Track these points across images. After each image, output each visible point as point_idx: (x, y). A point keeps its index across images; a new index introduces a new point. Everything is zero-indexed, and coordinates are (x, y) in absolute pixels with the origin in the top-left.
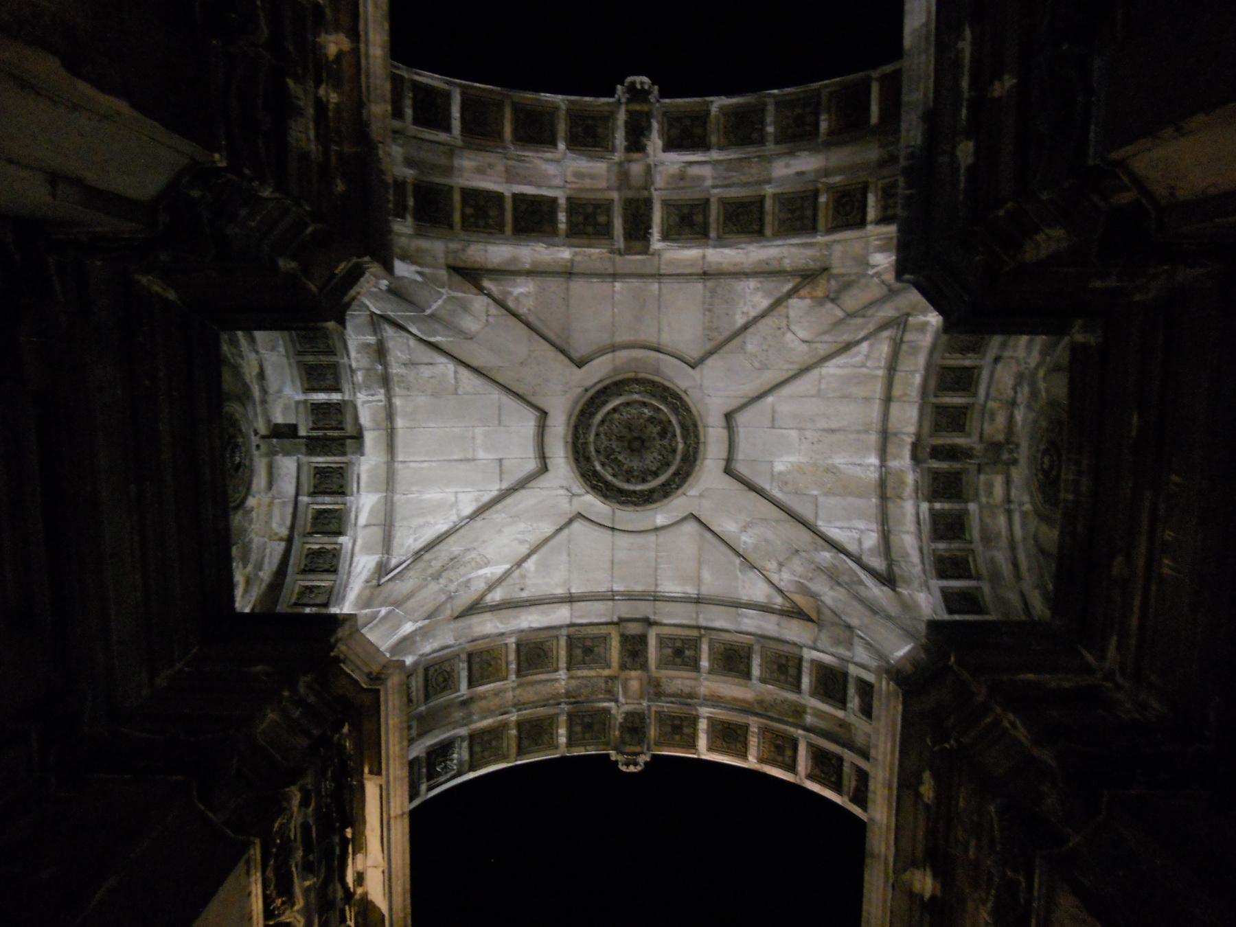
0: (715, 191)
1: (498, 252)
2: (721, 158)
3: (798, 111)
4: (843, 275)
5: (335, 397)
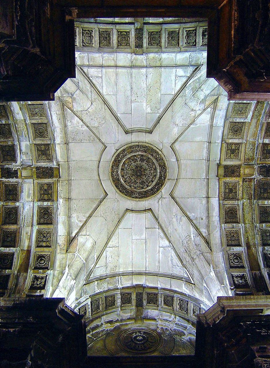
1: (61, 230)
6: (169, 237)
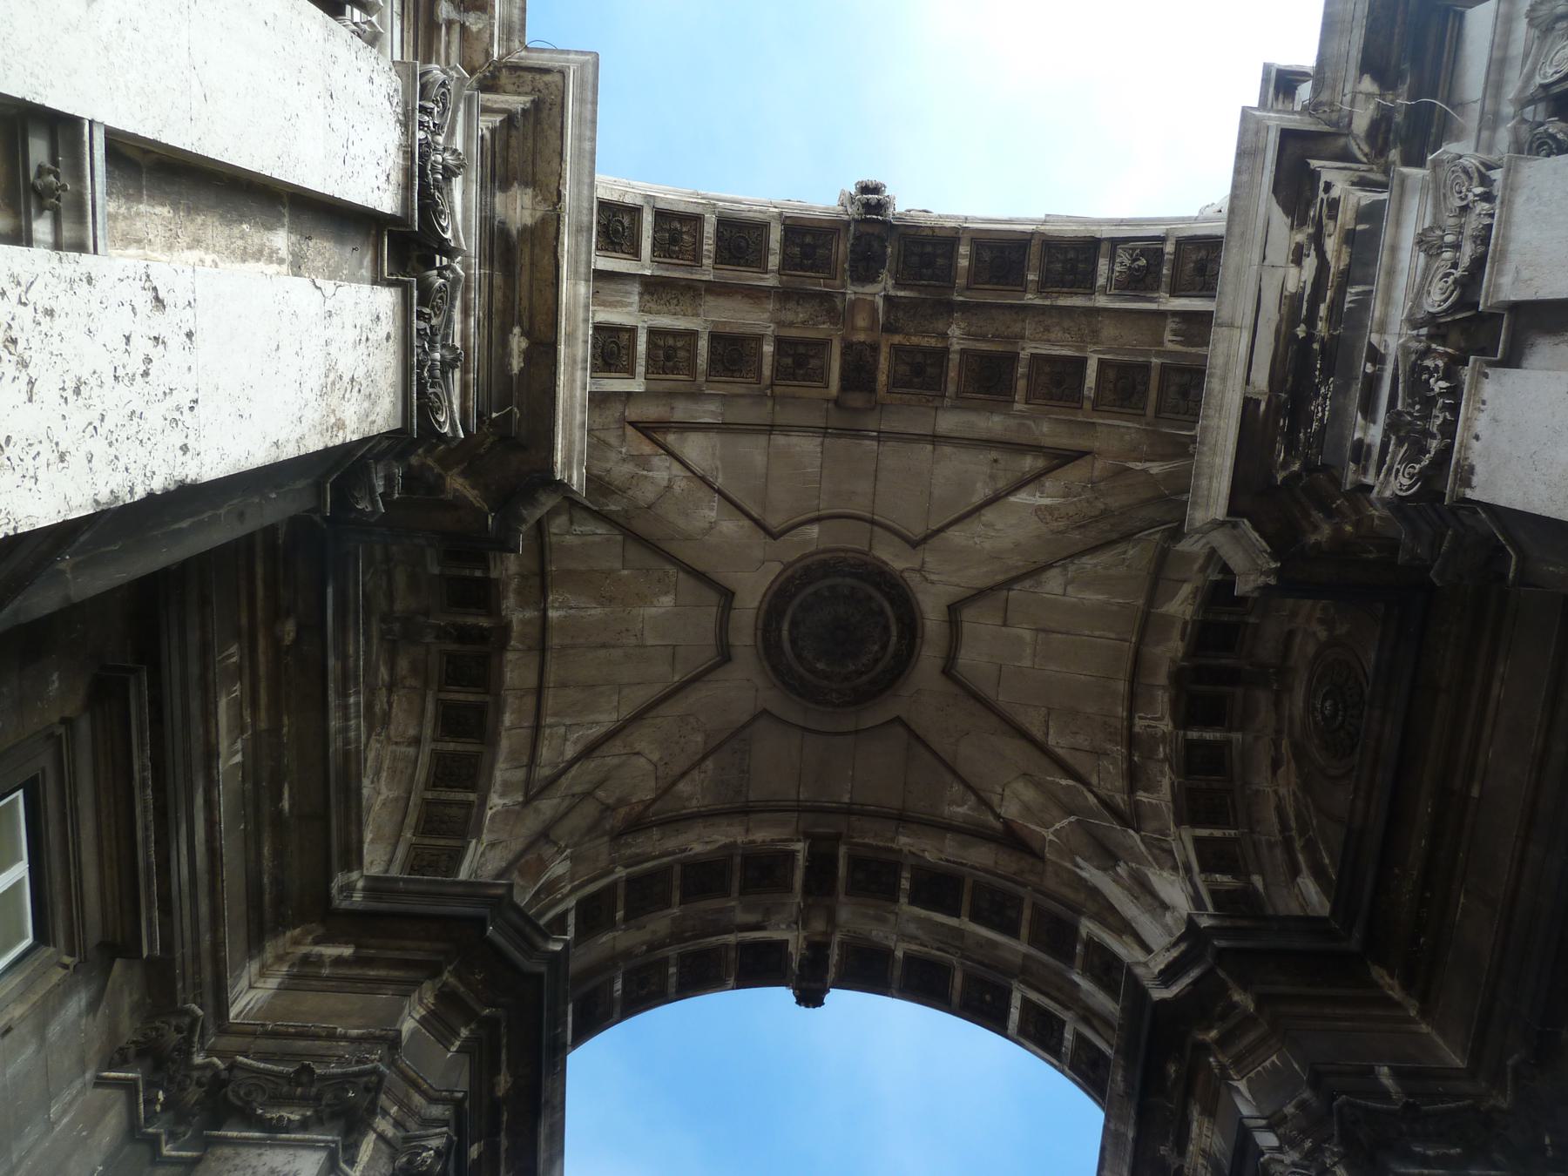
0: (733, 903)
1: (980, 856)
2: (726, 936)
6: (1034, 566)
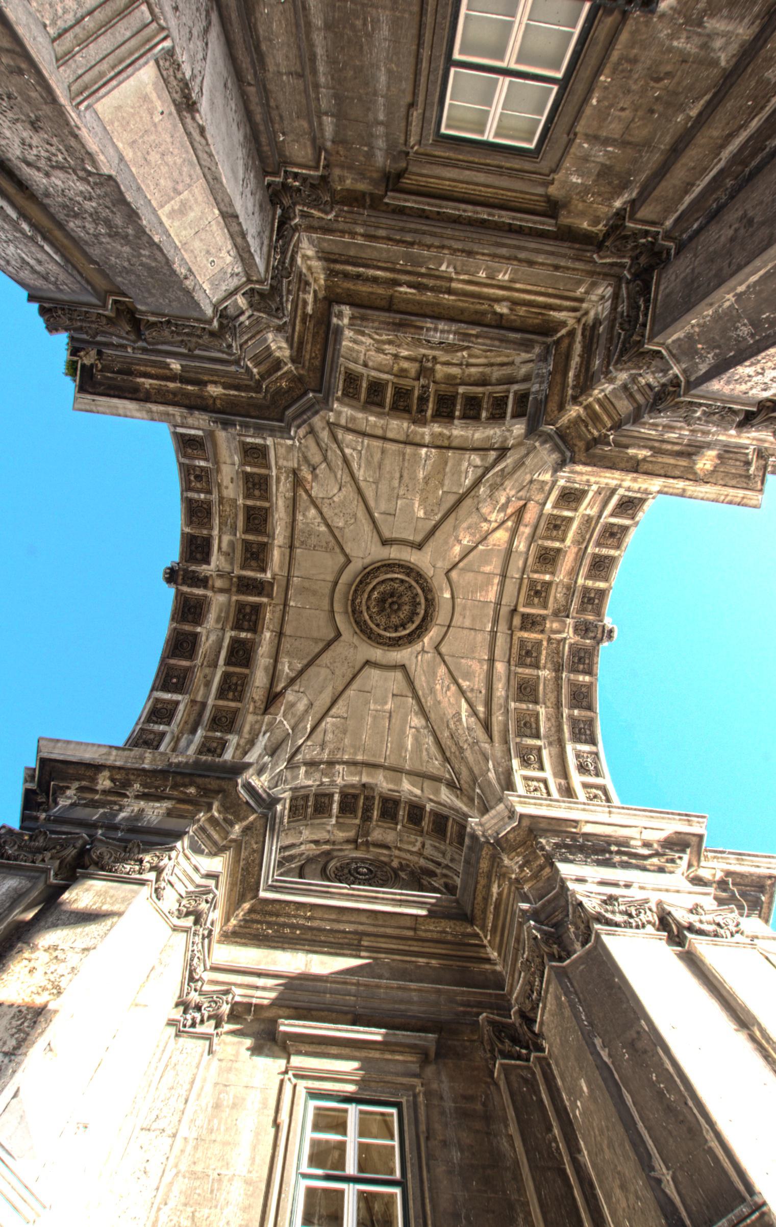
0: (238, 535)
1: (260, 679)
3: (192, 478)
4: (299, 461)
5: (336, 797)
